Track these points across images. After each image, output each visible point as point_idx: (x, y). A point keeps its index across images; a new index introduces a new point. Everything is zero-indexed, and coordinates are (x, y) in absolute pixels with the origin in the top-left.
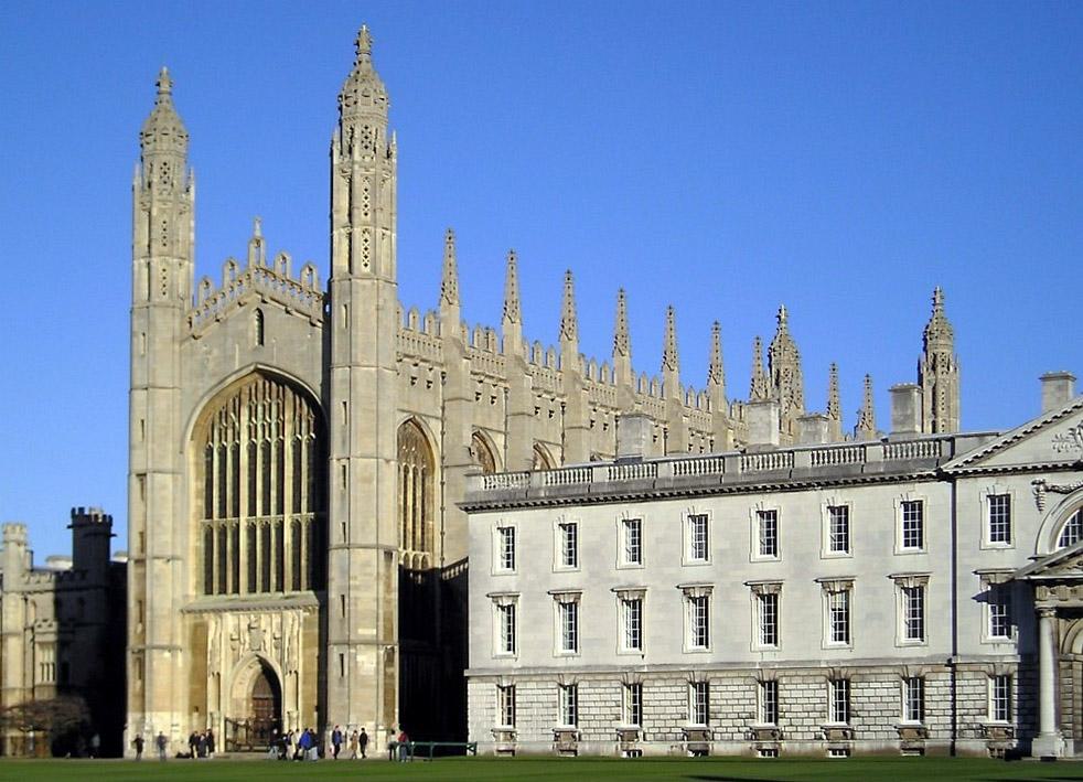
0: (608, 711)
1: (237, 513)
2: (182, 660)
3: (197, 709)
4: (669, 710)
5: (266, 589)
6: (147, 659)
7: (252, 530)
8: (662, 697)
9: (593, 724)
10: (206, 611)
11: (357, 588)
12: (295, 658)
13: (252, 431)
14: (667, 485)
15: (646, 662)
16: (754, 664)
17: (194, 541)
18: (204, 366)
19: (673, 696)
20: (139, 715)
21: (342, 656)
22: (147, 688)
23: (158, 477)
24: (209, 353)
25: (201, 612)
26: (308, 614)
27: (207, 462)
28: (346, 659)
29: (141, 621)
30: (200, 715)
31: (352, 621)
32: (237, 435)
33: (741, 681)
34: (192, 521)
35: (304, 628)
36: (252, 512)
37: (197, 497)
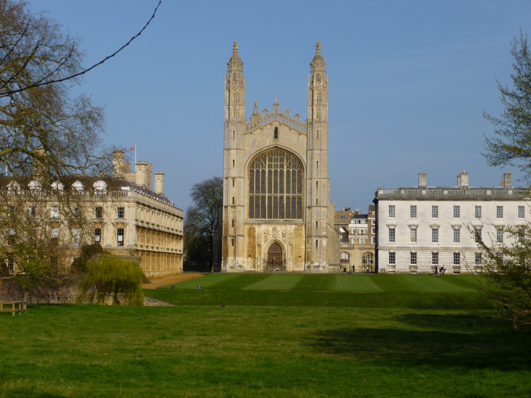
0: (427, 260)
1: (264, 192)
2: (246, 239)
3: (250, 256)
4: (447, 260)
5: (276, 217)
7: (270, 198)
8: (445, 257)
9: (422, 264)
11: (322, 219)
12: (292, 240)
13: (271, 166)
14: (447, 197)
15: (440, 246)
16: (475, 248)
17: (247, 201)
19: (449, 257)
20: (233, 258)
21: (317, 241)
22: (237, 249)
23: (240, 179)
24: (257, 139)
25: (252, 224)
27: (250, 175)
28: (319, 242)
29: (233, 226)
30: (252, 258)
31: (321, 230)
32: (264, 167)
33: (470, 253)
34: (247, 194)
35: (295, 231)
36: (270, 192)
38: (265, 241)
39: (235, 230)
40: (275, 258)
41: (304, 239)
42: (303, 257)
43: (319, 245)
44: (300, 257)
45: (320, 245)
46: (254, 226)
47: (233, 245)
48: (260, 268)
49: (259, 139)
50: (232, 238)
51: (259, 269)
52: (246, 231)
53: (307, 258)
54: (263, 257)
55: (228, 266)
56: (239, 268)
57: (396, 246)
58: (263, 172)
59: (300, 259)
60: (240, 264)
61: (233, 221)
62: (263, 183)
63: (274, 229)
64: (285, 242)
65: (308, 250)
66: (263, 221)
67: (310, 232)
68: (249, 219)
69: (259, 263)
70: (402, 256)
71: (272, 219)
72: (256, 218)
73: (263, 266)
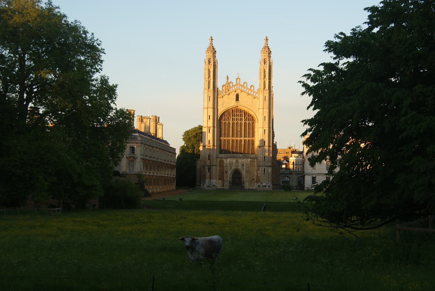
3: (220, 179)
6: (211, 168)
10: (223, 158)
18: (223, 104)
20: (209, 180)
21: (264, 169)
22: (211, 174)
25: (222, 158)
26: (251, 159)
28: (266, 170)
29: (209, 159)
30: (221, 180)
37: (219, 133)
38: (230, 169)
39: (210, 162)
40: (237, 180)
41: (256, 168)
42: (255, 180)
43: (266, 172)
44: (253, 179)
45: (267, 171)
46: (223, 159)
47: (209, 172)
48: (227, 187)
49: (226, 102)
50: (208, 167)
51: (226, 188)
52: (218, 162)
53: (258, 181)
54: (229, 180)
55: (206, 185)
56: (213, 187)
57: (317, 172)
58: (229, 123)
59: (253, 181)
60: (214, 184)
61: (209, 156)
62: (229, 131)
63: (237, 161)
64: (243, 170)
65: (259, 175)
66: (229, 156)
67: (260, 163)
68: (220, 155)
69: (226, 184)
70: (320, 179)
71: (236, 155)
72: (224, 154)
73: (229, 186)
